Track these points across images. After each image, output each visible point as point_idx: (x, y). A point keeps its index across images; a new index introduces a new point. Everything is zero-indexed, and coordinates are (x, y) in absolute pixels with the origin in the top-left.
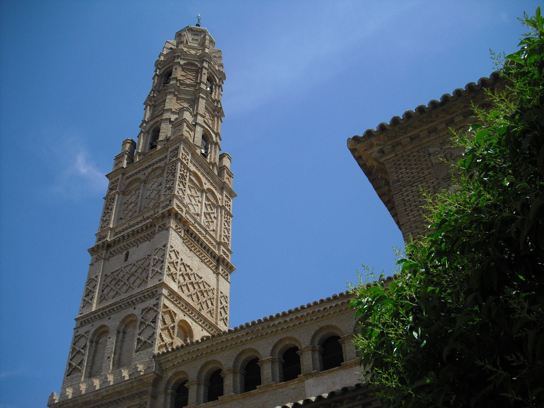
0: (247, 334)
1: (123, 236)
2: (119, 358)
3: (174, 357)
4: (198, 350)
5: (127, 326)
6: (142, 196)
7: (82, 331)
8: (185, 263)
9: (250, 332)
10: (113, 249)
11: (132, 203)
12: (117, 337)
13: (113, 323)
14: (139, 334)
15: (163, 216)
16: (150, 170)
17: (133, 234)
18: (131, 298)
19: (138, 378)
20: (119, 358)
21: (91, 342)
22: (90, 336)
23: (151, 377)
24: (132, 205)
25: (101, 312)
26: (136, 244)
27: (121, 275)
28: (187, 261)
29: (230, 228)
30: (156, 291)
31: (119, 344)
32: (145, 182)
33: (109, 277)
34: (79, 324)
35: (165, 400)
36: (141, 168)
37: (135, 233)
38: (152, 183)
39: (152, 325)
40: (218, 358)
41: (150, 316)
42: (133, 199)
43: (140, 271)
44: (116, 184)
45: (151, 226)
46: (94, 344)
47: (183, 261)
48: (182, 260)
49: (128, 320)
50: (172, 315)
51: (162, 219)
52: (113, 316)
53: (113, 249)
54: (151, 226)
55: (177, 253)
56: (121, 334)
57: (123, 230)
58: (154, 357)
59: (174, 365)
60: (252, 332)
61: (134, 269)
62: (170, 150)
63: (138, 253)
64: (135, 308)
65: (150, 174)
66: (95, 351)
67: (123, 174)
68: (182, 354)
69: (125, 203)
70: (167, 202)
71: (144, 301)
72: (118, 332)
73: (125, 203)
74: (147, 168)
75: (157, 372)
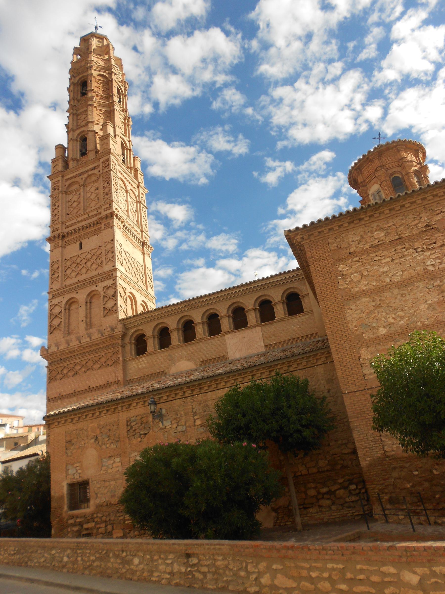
0: (185, 306)
1: (75, 230)
2: (90, 321)
5: (91, 298)
7: (55, 301)
12: (86, 306)
13: (81, 296)
15: (107, 217)
16: (86, 175)
17: (83, 229)
20: (90, 321)
21: (65, 309)
22: (63, 305)
26: (88, 236)
27: (79, 260)
28: (127, 250)
30: (112, 274)
31: (88, 310)
32: (84, 185)
33: (69, 262)
34: (51, 296)
35: (131, 348)
36: (77, 173)
37: (85, 228)
38: (90, 187)
40: (165, 321)
41: (111, 292)
42: (75, 198)
43: (94, 258)
44: (58, 185)
45: (98, 223)
46: (67, 311)
49: (93, 294)
56: (88, 304)
57: (73, 224)
58: (120, 320)
61: (89, 256)
62: (101, 160)
63: (91, 243)
65: (86, 178)
66: (69, 316)
69: (69, 201)
70: (108, 206)
72: (86, 303)
73: (69, 201)
74: (82, 173)
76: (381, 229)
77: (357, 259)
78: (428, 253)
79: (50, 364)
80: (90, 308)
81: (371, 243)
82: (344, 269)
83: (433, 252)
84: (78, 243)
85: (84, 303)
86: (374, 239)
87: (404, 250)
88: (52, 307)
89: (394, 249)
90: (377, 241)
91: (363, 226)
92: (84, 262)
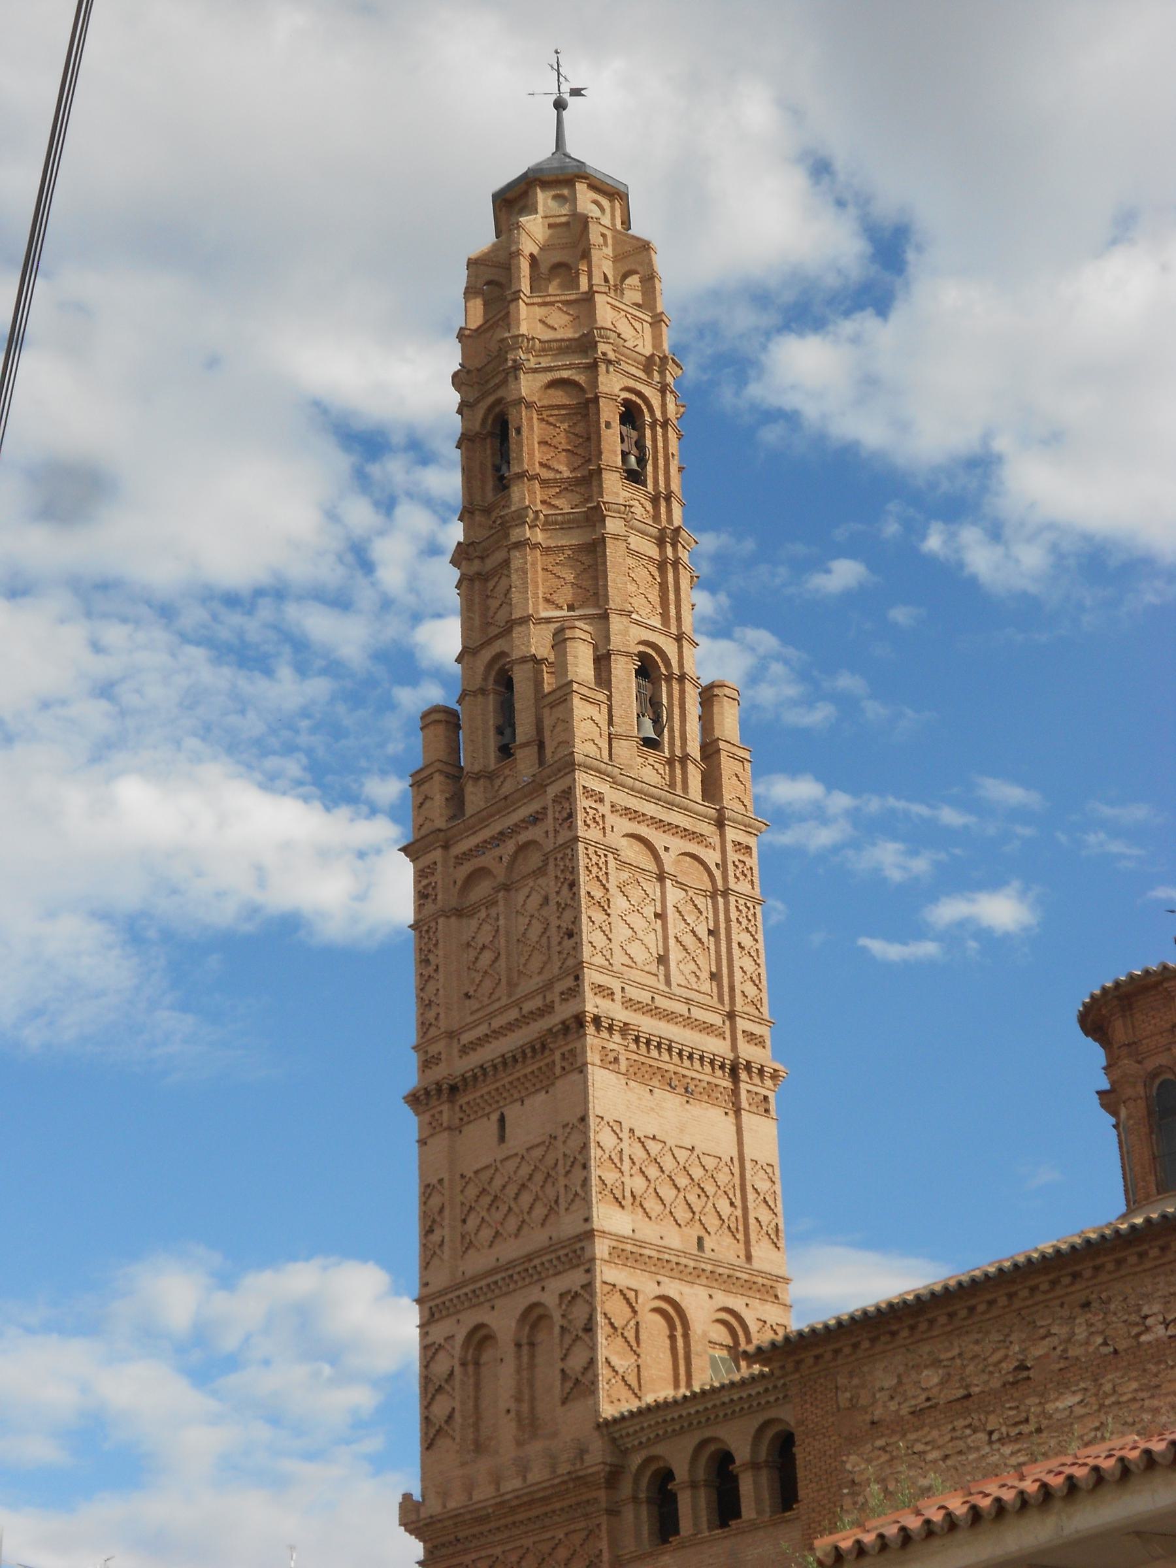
0: (766, 1390)
2: (532, 1409)
3: (638, 1428)
4: (681, 1416)
5: (534, 1327)
6: (508, 933)
7: (438, 1332)
8: (641, 1136)
9: (770, 1387)
10: (466, 1099)
11: (484, 947)
12: (519, 1357)
13: (503, 1320)
14: (562, 1359)
15: (565, 1028)
16: (510, 846)
17: (505, 1064)
18: (531, 1260)
19: (574, 1476)
20: (532, 1409)
21: (463, 1364)
22: (457, 1351)
23: (598, 1473)
24: (487, 956)
25: (472, 1287)
27: (498, 1182)
29: (761, 946)
30: (582, 1249)
31: (525, 1374)
34: (427, 1313)
35: (637, 1517)
37: (509, 1061)
38: (526, 890)
39: (585, 1337)
41: (579, 1312)
42: (485, 937)
43: (539, 1178)
44: (432, 879)
46: (471, 1368)
47: (637, 1133)
48: (632, 1130)
50: (629, 1298)
51: (565, 1035)
52: (498, 1303)
53: (466, 1099)
54: (544, 1047)
55: (616, 1127)
56: (525, 1349)
59: (641, 1443)
60: (775, 1387)
61: (525, 1170)
63: (530, 1120)
64: (543, 1288)
66: (477, 1386)
67: (446, 847)
68: (653, 1423)
69: (468, 945)
70: (569, 982)
71: (559, 1273)
72: (518, 1345)
74: (502, 837)
75: (609, 1460)
76: (936, 1363)
77: (880, 1443)
78: (1007, 1450)
79: (429, 1552)
80: (532, 1366)
81: (913, 1402)
82: (857, 1469)
83: (1017, 1447)
84: (495, 1117)
85: (511, 1349)
86: (919, 1391)
87: (968, 1432)
88: (430, 1353)
89: (950, 1427)
90: (923, 1397)
91: (903, 1350)
92: (512, 1190)
